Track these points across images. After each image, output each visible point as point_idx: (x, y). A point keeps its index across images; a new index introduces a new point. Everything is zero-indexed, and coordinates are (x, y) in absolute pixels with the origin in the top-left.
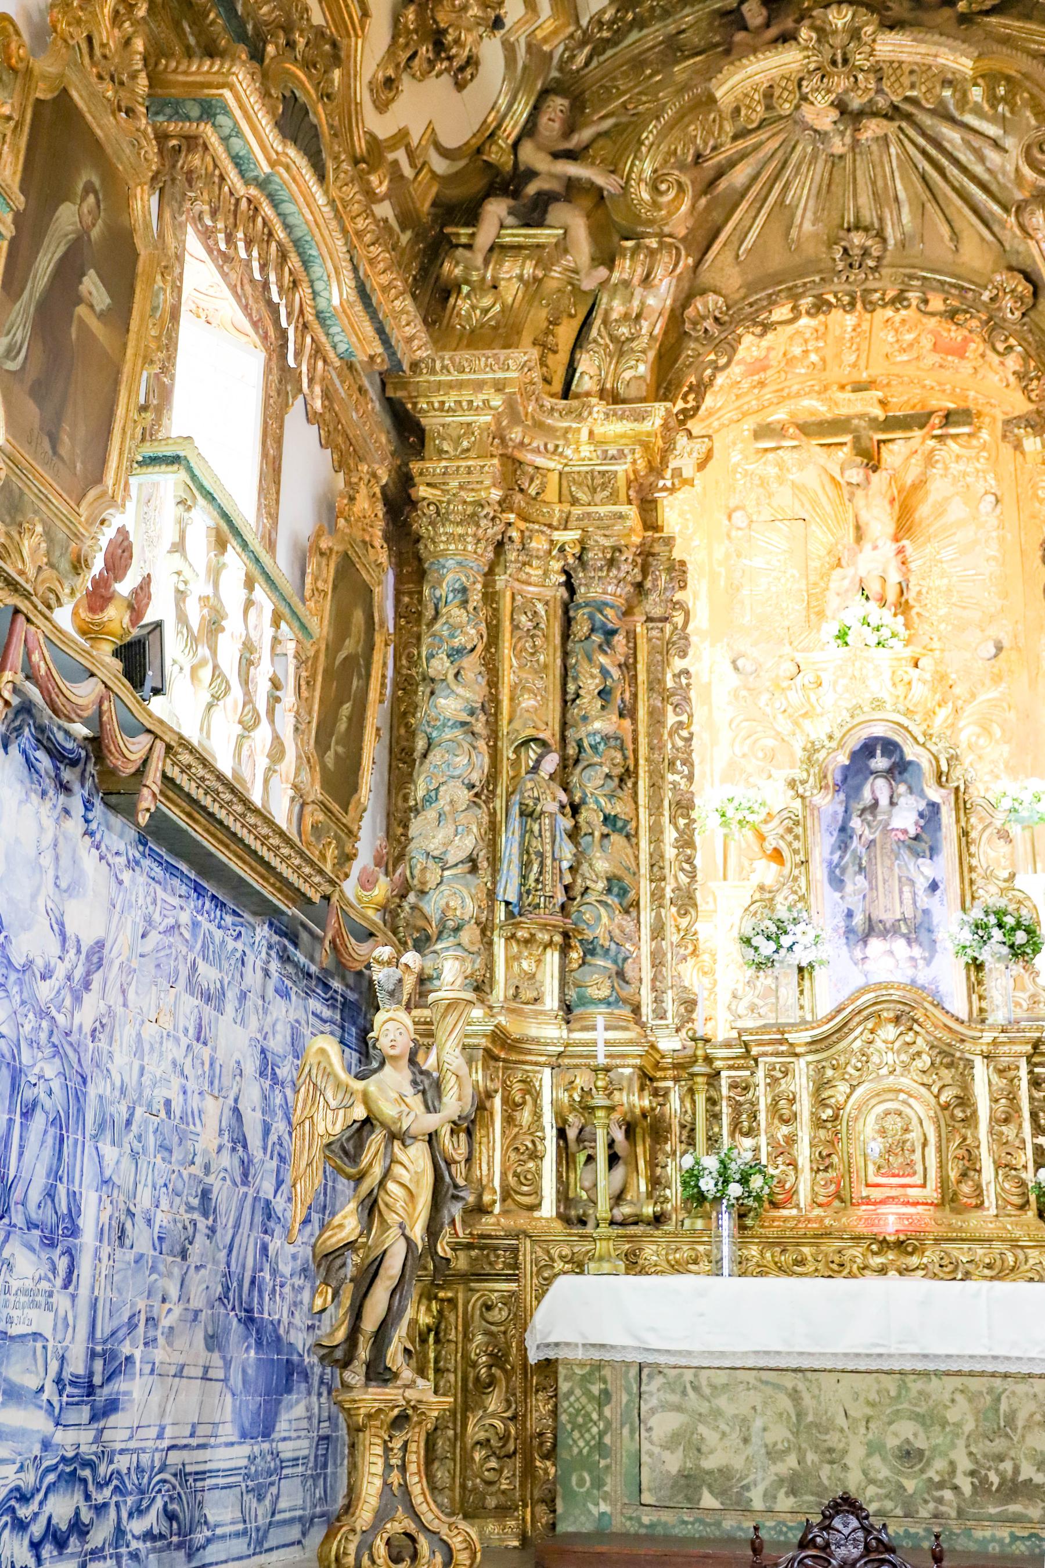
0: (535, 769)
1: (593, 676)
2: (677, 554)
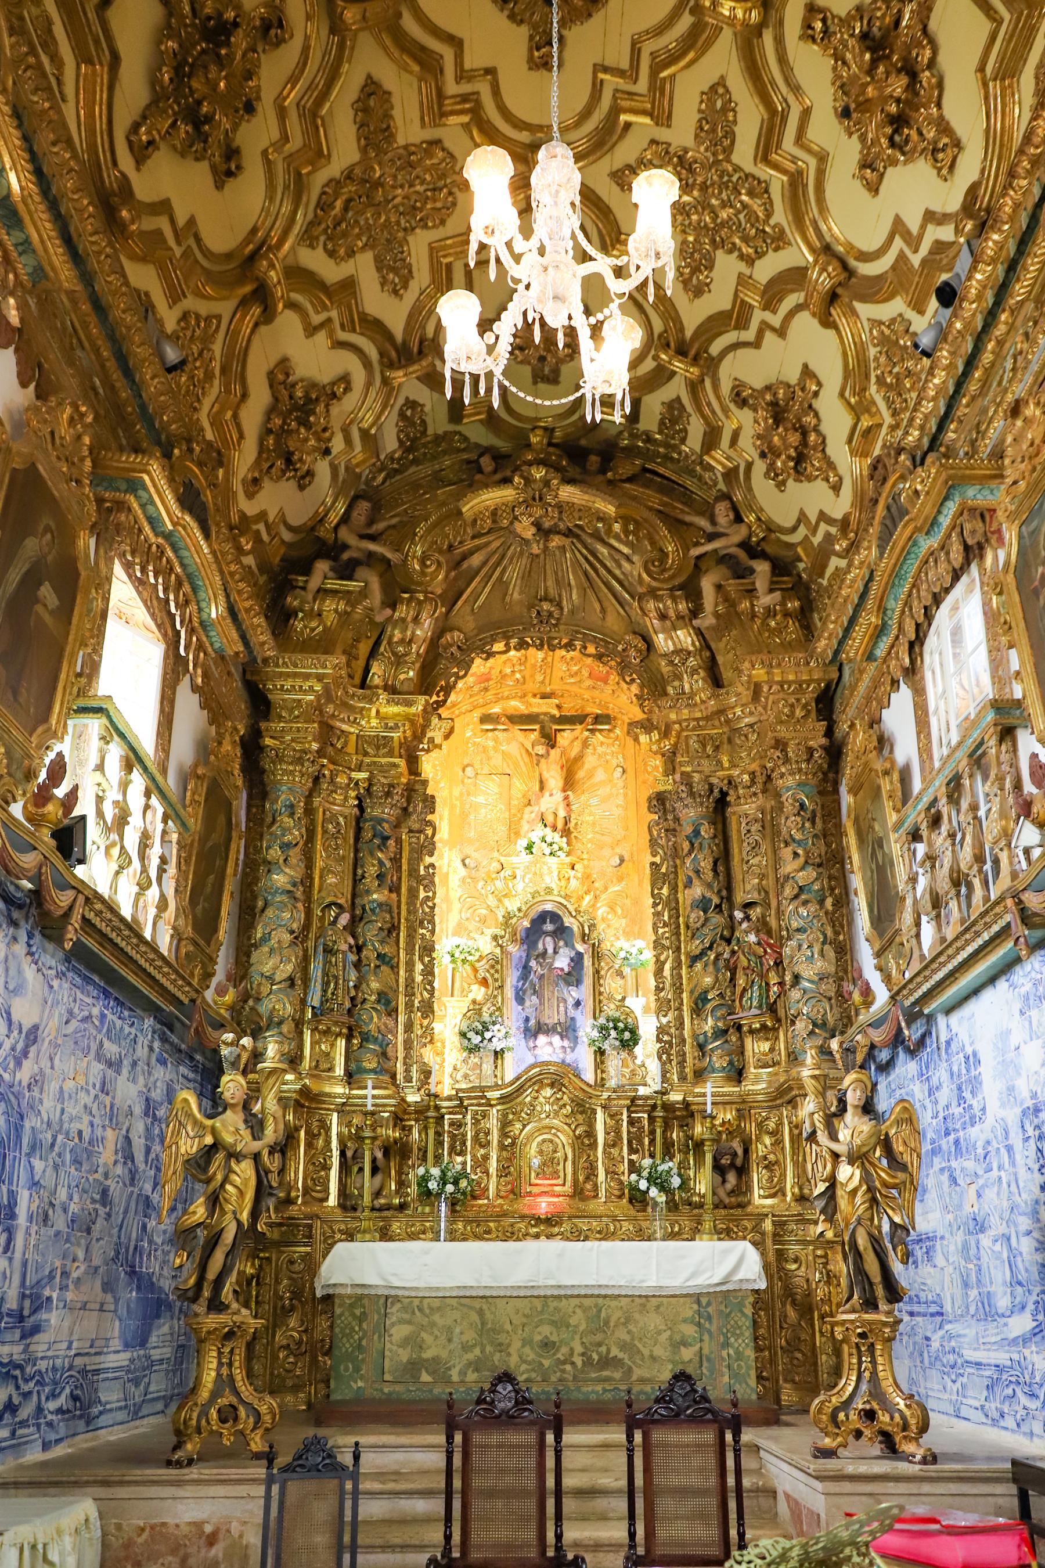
2: (429, 792)
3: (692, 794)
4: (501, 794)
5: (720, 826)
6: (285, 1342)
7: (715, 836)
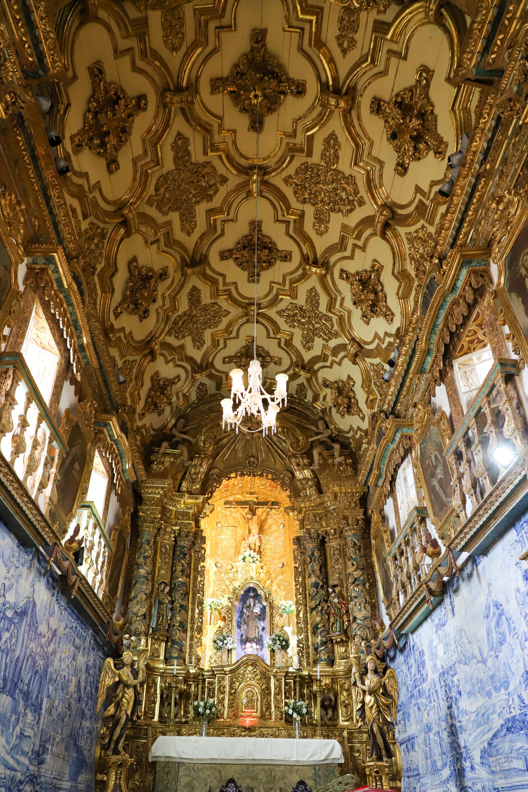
3: (311, 538)
5: (323, 552)
7: (320, 556)
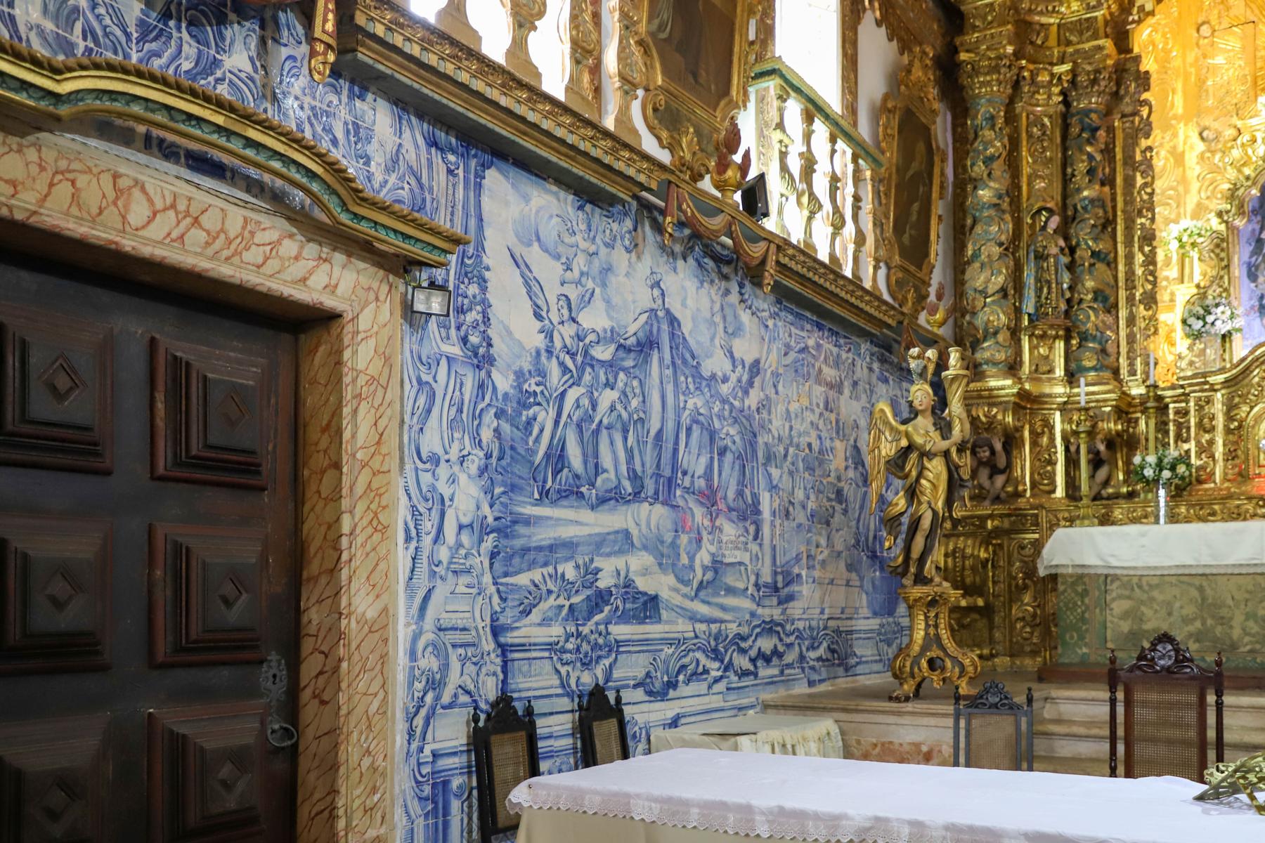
0: (1044, 228)
1: (1083, 161)
2: (1143, 68)
4: (1244, 48)
6: (1021, 615)
